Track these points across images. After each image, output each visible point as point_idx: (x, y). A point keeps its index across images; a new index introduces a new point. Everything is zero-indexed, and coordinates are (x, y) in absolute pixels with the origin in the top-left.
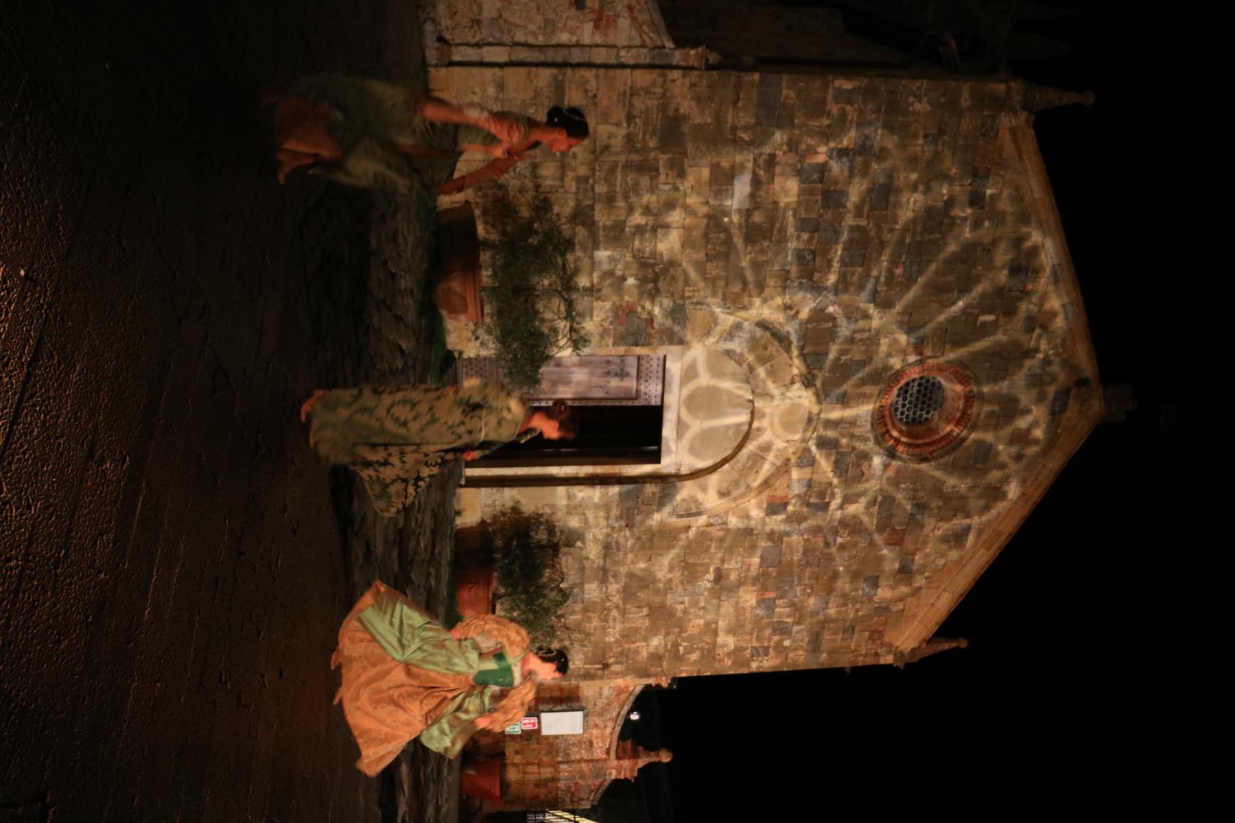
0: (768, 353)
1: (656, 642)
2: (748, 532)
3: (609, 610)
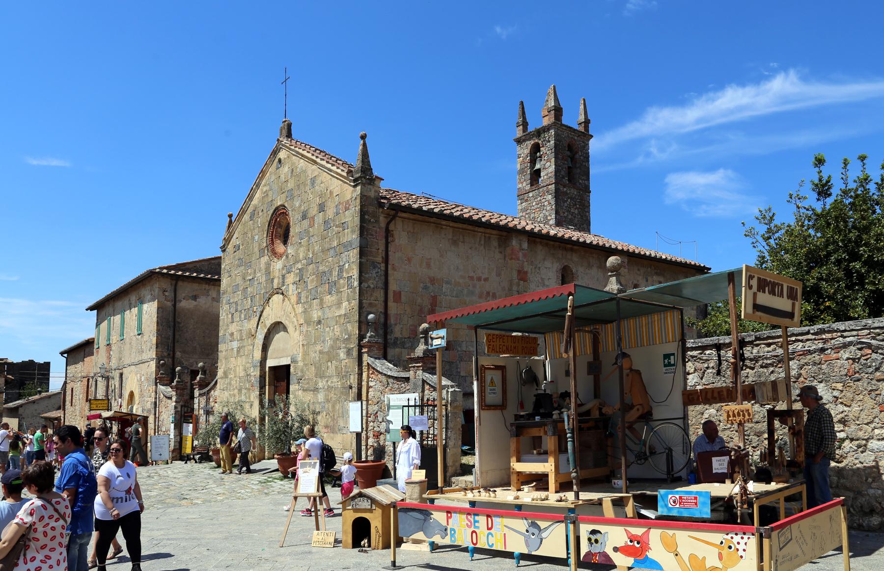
2: (305, 312)
3: (329, 387)
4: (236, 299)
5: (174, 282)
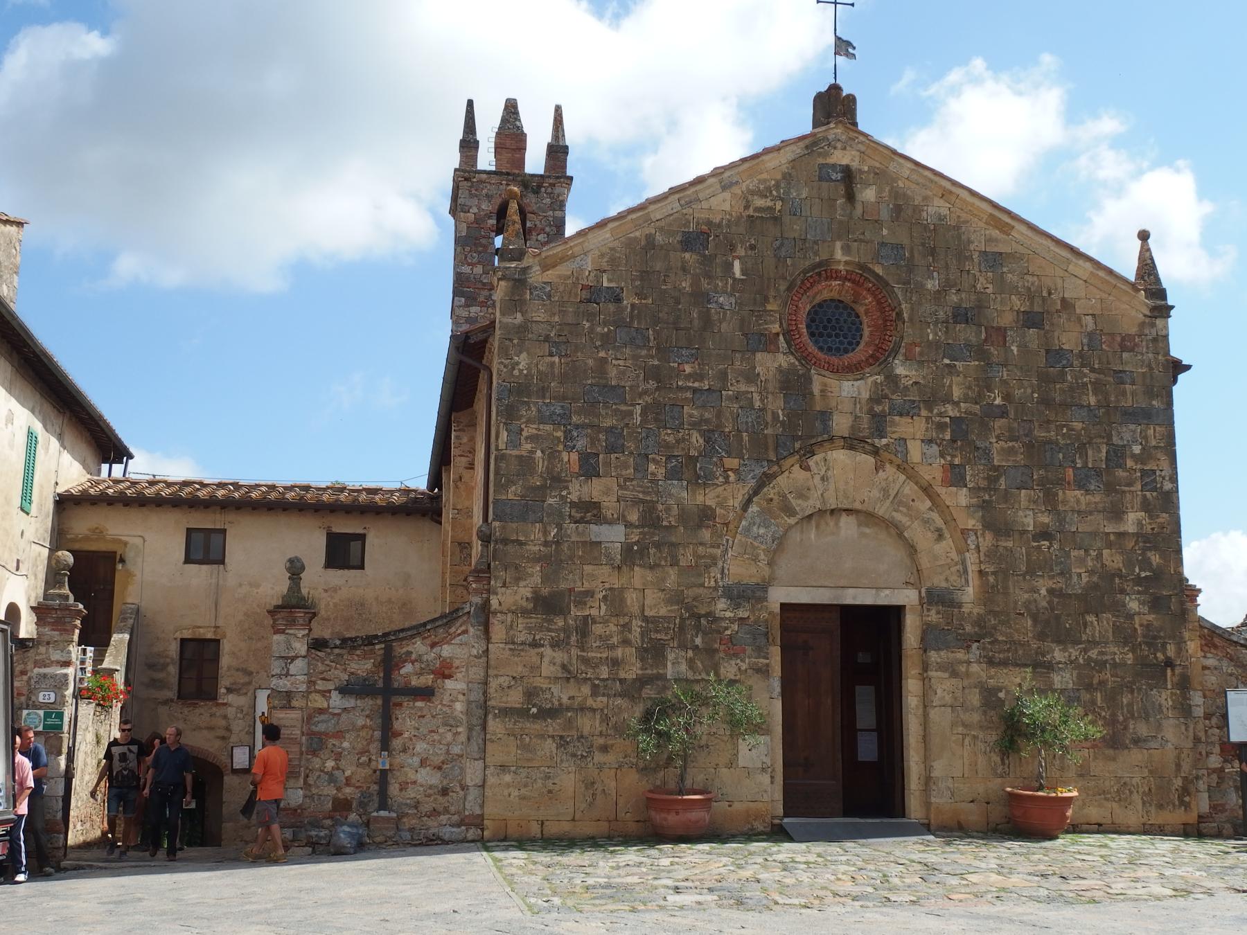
0: (776, 497)
1: (1134, 605)
2: (985, 506)
4: (608, 423)
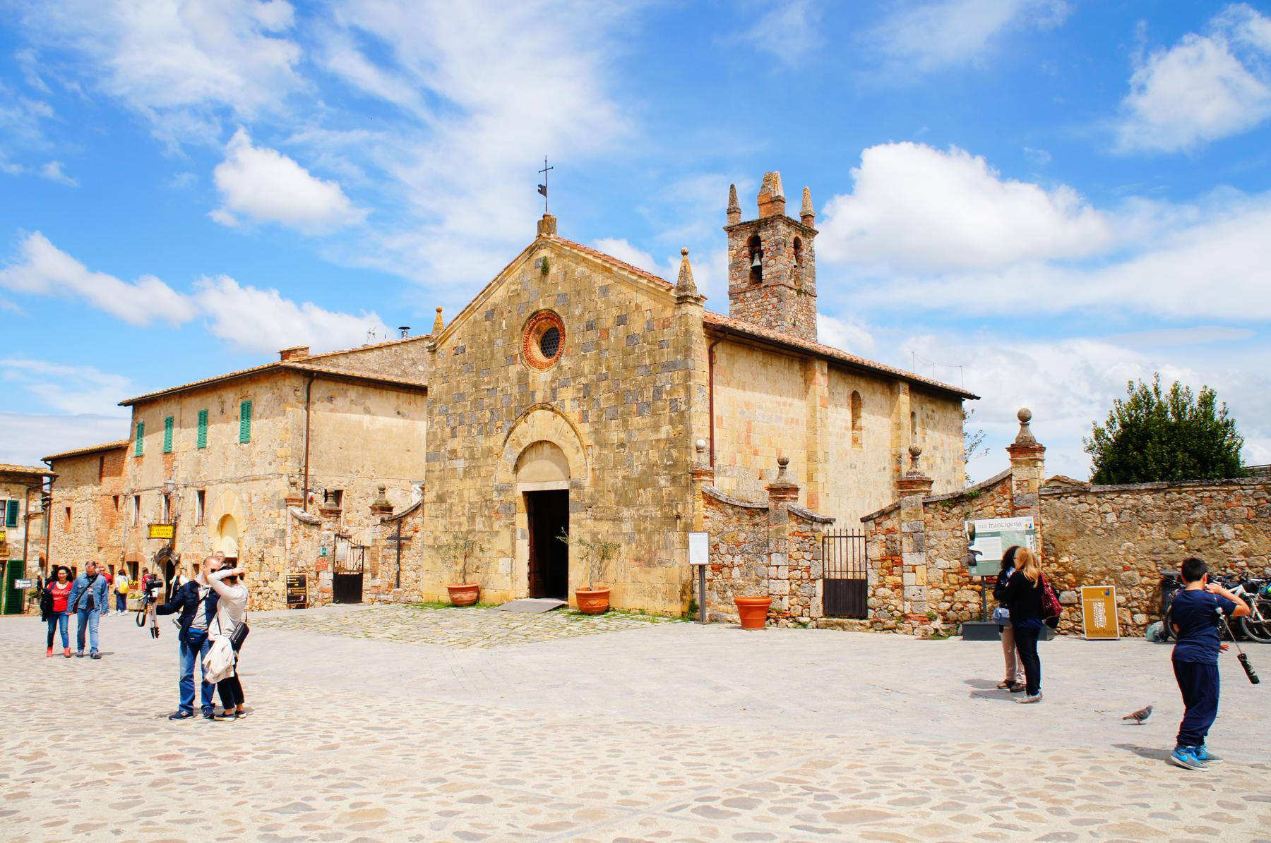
1: (663, 482)
2: (596, 432)
5: (307, 380)
